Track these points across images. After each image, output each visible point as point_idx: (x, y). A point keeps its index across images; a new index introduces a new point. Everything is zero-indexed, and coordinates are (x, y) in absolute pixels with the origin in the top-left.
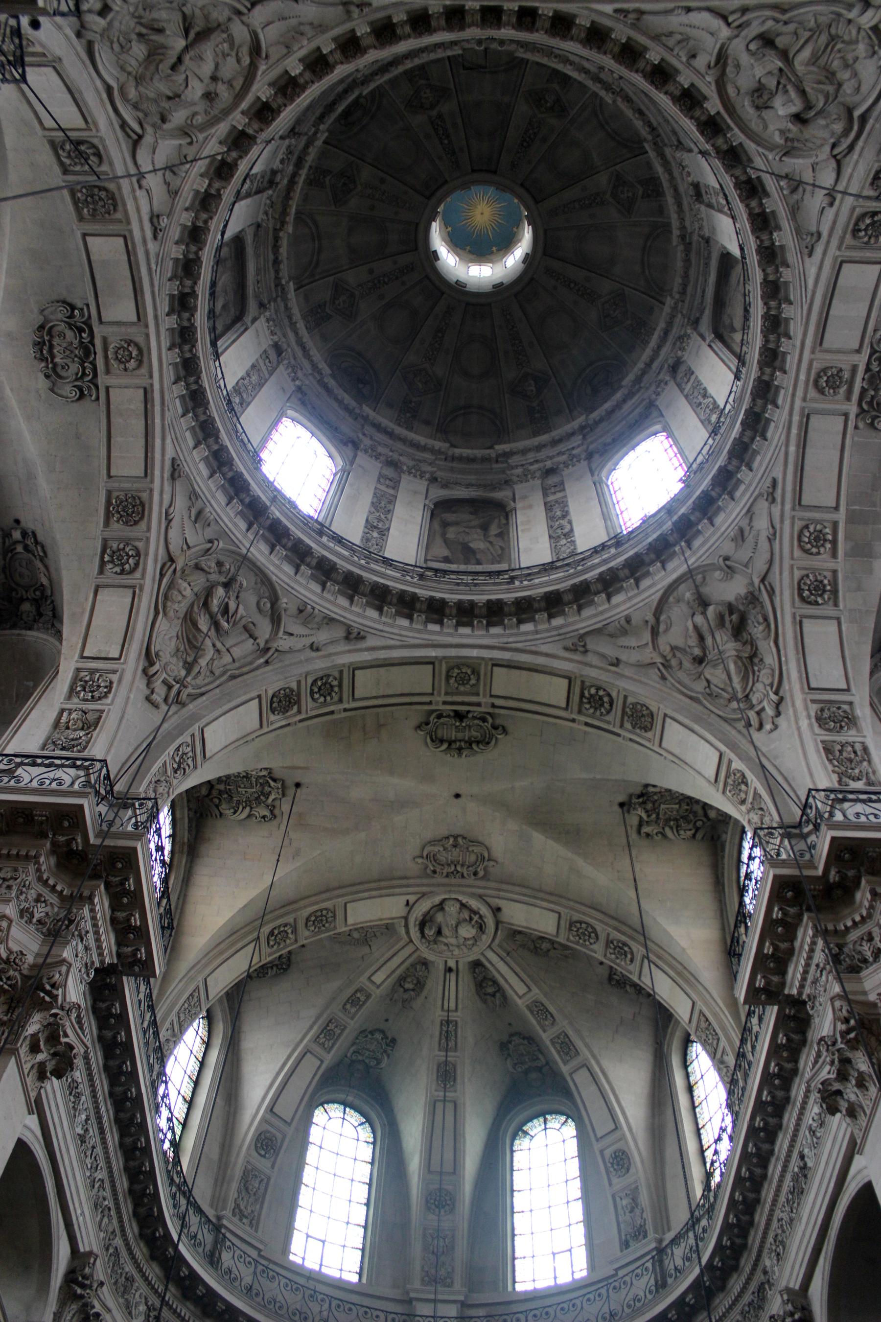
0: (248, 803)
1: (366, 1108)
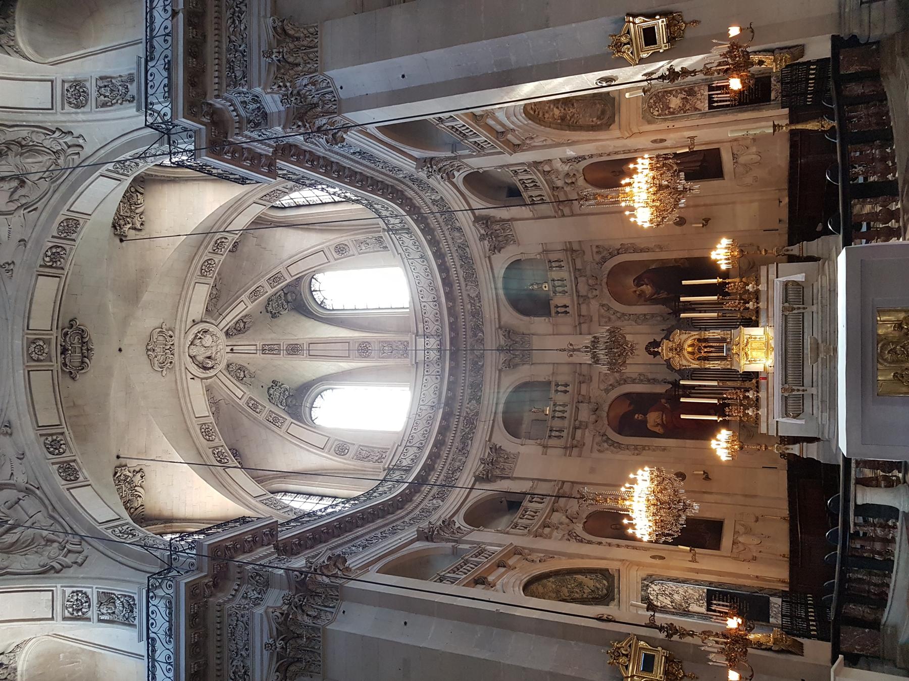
0: (133, 489)
1: (313, 395)
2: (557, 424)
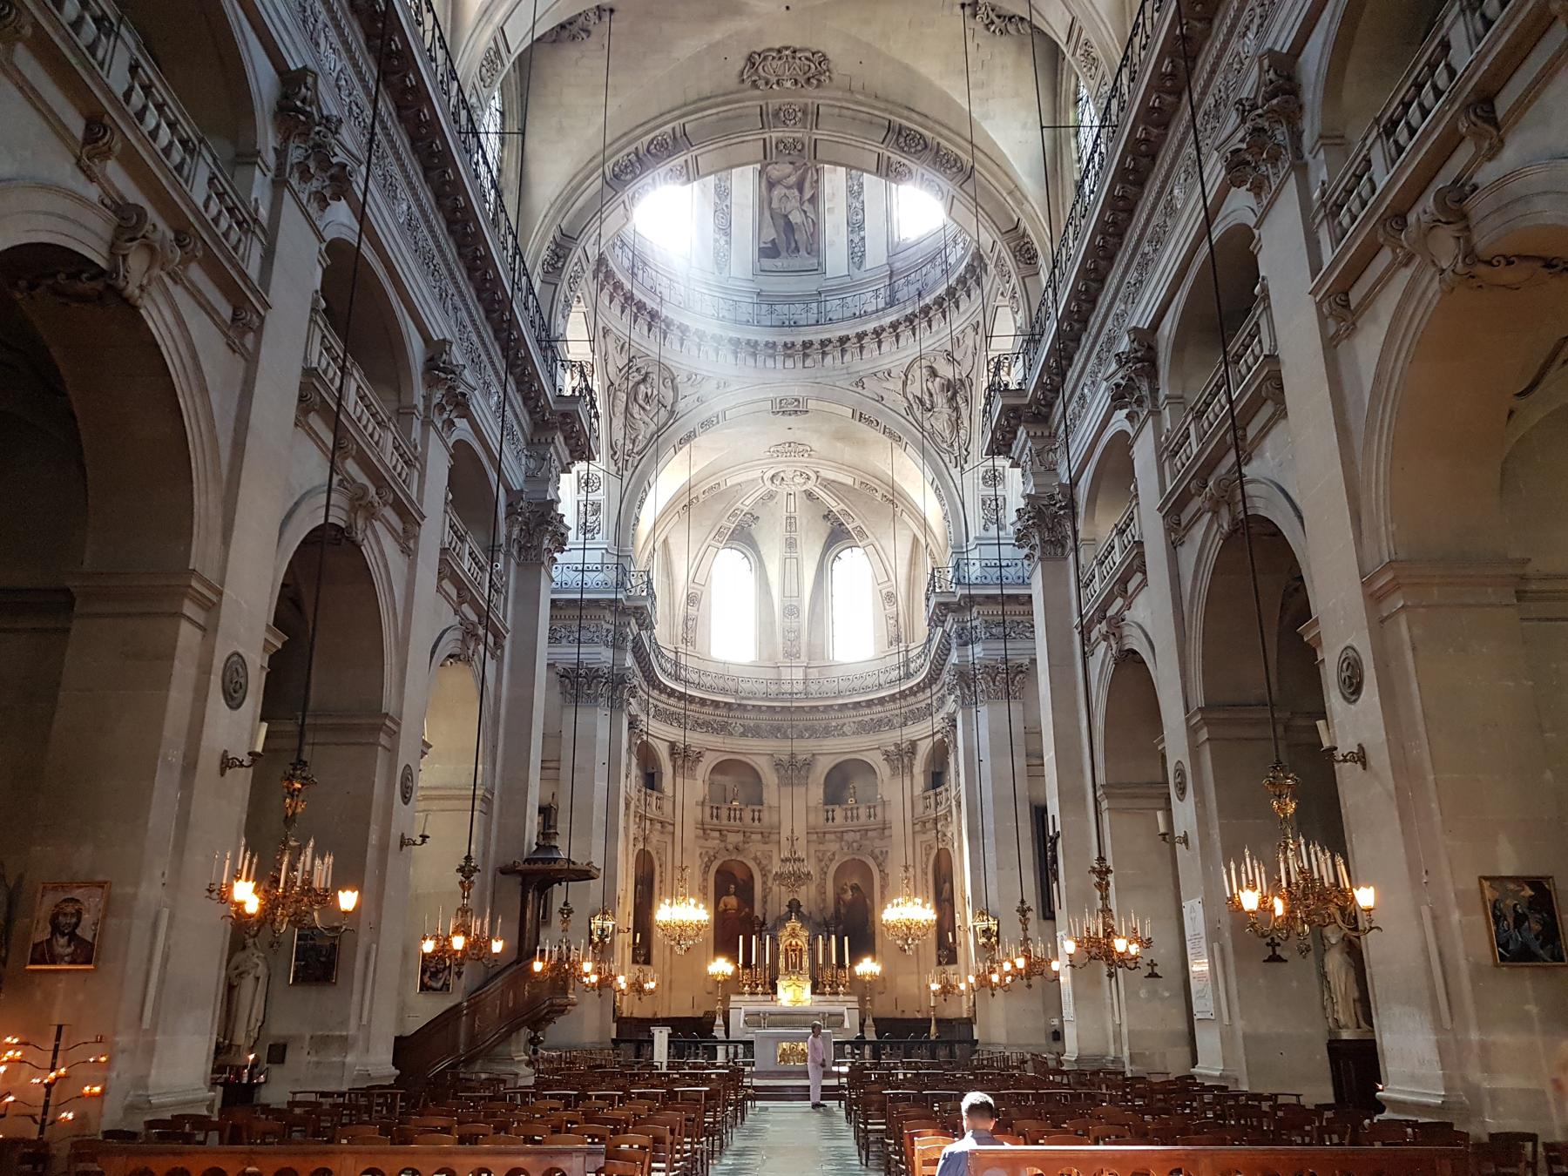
2: (724, 813)
